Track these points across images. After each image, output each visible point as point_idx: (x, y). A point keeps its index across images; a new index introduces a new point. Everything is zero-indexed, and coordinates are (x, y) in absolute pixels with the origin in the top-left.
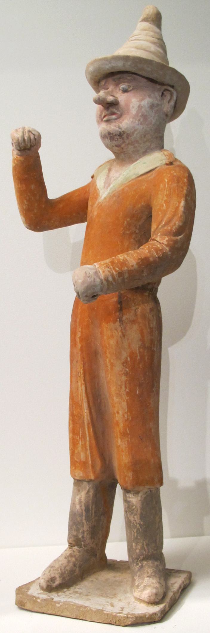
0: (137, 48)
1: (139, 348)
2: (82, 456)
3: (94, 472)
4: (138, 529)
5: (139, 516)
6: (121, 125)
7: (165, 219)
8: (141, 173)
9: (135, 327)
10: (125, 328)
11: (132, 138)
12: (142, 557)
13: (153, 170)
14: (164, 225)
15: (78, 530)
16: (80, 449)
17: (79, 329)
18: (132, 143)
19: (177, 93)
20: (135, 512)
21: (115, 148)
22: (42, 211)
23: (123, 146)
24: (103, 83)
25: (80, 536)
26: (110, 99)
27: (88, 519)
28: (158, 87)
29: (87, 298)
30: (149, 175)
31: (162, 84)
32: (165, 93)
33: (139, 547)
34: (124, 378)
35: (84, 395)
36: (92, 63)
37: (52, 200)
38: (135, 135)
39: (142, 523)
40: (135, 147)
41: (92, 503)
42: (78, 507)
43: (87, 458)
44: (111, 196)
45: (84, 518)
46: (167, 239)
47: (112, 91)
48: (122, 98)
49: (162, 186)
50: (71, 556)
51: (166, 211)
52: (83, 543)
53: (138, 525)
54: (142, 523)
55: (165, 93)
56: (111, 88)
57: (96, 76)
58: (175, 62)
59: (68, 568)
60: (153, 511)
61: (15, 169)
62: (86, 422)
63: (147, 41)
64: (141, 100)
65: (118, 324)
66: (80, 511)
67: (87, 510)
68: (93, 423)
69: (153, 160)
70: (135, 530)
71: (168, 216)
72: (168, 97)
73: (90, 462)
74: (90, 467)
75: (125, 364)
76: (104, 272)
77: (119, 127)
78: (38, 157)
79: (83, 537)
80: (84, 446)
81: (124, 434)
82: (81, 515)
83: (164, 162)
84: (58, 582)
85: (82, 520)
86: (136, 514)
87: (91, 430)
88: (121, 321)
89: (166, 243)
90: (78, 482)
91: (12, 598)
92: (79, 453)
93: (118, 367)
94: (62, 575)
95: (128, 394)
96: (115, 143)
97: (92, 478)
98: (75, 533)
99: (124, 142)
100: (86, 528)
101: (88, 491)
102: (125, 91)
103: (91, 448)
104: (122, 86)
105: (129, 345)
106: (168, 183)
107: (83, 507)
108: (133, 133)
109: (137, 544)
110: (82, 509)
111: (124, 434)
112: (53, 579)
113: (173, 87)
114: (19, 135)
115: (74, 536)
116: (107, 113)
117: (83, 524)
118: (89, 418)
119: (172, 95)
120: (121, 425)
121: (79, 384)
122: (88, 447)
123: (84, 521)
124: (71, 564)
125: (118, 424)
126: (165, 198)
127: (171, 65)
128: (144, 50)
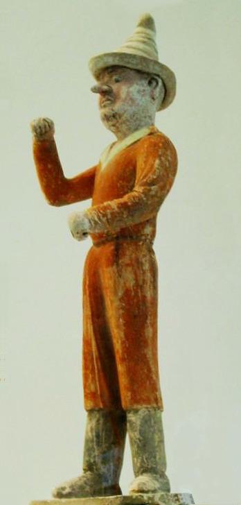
0: (128, 47)
1: (133, 286)
2: (92, 388)
3: (103, 402)
5: (138, 432)
6: (114, 108)
7: (144, 175)
9: (130, 269)
10: (121, 271)
11: (123, 118)
12: (142, 469)
13: (138, 140)
15: (90, 455)
16: (90, 381)
18: (124, 122)
21: (112, 128)
22: (59, 189)
23: (117, 125)
24: (101, 77)
25: (92, 461)
26: (105, 88)
27: (99, 444)
29: (79, 235)
31: (148, 74)
33: (139, 460)
34: (121, 312)
35: (92, 334)
38: (125, 115)
39: (141, 438)
40: (128, 126)
41: (103, 430)
42: (90, 434)
43: (96, 388)
44: (109, 165)
45: (95, 443)
46: (143, 188)
47: (107, 82)
48: (115, 87)
49: (142, 150)
50: (84, 477)
51: (145, 167)
52: (95, 467)
53: (138, 441)
54: (141, 438)
56: (106, 79)
58: (167, 56)
59: (79, 483)
60: (152, 430)
61: (35, 152)
64: (129, 88)
65: (114, 267)
66: (91, 437)
67: (98, 436)
68: (100, 357)
69: (142, 133)
70: (136, 446)
72: (154, 84)
73: (99, 393)
74: (99, 397)
75: (121, 300)
76: (91, 213)
77: (113, 110)
78: (53, 141)
79: (95, 462)
80: (93, 378)
81: (123, 360)
82: (92, 441)
84: (68, 490)
85: (93, 446)
86: (136, 431)
88: (118, 265)
89: (141, 191)
90: (91, 411)
92: (89, 385)
93: (117, 303)
94: (72, 487)
95: (125, 325)
96: (111, 123)
97: (102, 406)
98: (87, 459)
99: (118, 122)
100: (96, 453)
101: (98, 421)
102: (117, 81)
103: (99, 381)
104: (115, 77)
105: (125, 283)
106: (147, 148)
107: (94, 434)
108: (123, 114)
109: (137, 458)
110: (92, 436)
111: (123, 360)
112: (63, 489)
114: (35, 123)
115: (87, 461)
118: (97, 353)
119: (157, 83)
120: (120, 351)
121: (89, 325)
122: (97, 379)
123: (95, 447)
124: (82, 482)
125: (118, 352)
126: (144, 159)
127: (161, 61)
128: (134, 48)
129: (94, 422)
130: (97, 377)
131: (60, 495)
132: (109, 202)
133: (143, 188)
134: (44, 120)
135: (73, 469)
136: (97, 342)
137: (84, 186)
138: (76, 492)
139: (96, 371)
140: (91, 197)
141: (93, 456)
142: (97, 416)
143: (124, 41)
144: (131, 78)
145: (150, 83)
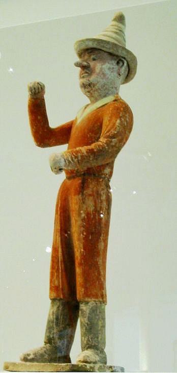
0: (104, 35)
1: (93, 212)
2: (56, 283)
3: (63, 294)
4: (86, 328)
5: (87, 318)
6: (90, 79)
7: (107, 130)
8: (98, 107)
9: (91, 198)
10: (85, 199)
11: (96, 87)
12: (87, 346)
13: (106, 104)
14: (107, 132)
15: (50, 333)
16: (55, 278)
17: (60, 201)
18: (97, 90)
19: (127, 61)
20: (85, 316)
21: (87, 93)
22: (45, 135)
23: (91, 92)
24: (82, 55)
25: (51, 336)
26: (85, 64)
27: (57, 324)
28: (115, 57)
29: (56, 170)
30: (104, 107)
31: (117, 56)
32: (120, 62)
34: (82, 229)
35: (60, 243)
36: (76, 44)
37: (53, 129)
38: (98, 85)
40: (99, 93)
41: (61, 315)
42: (51, 317)
43: (59, 283)
44: (83, 121)
45: (54, 324)
46: (106, 139)
47: (87, 60)
48: (92, 64)
49: (108, 112)
50: (44, 347)
51: (109, 125)
52: (53, 341)
55: (120, 62)
56: (86, 57)
57: (79, 51)
58: (131, 45)
59: (40, 352)
60: (97, 317)
61: (29, 107)
63: (112, 32)
64: (102, 65)
65: (80, 195)
66: (52, 319)
67: (57, 319)
68: (64, 261)
69: (109, 99)
70: (84, 328)
71: (109, 128)
72: (121, 64)
73: (61, 287)
74: (61, 290)
75: (83, 220)
76: (66, 155)
77: (89, 80)
78: (44, 100)
79: (53, 337)
80: (58, 276)
81: (81, 264)
82: (53, 322)
83: (113, 100)
84: (32, 356)
85: (53, 325)
86: (85, 317)
87: (63, 266)
88: (83, 194)
89: (105, 142)
90: (53, 300)
91: (3, 366)
92: (54, 280)
93: (80, 222)
94: (35, 354)
95: (84, 239)
96: (87, 90)
97: (62, 297)
99: (92, 89)
100: (55, 331)
101: (58, 307)
102: (94, 60)
103: (62, 278)
105: (87, 208)
106: (112, 110)
107: (55, 317)
108: (96, 84)
109: (85, 338)
111: (81, 264)
112: (29, 355)
113: (125, 58)
114: (31, 85)
115: (48, 337)
116: (83, 72)
117: (54, 327)
118: (62, 258)
119: (123, 64)
120: (79, 258)
121: (58, 237)
122: (60, 277)
123: (54, 326)
124: (43, 351)
125: (77, 257)
126: (109, 119)
127: (126, 48)
128: (109, 36)
129: (55, 308)
130: (60, 275)
131: (25, 359)
132: (81, 148)
133: (106, 139)
134: (38, 83)
135: (37, 341)
136: (62, 250)
137: (63, 134)
138: (37, 358)
139: (60, 271)
140: (68, 143)
141: (52, 333)
142: (58, 304)
143: (102, 31)
144: (105, 58)
145: (118, 63)
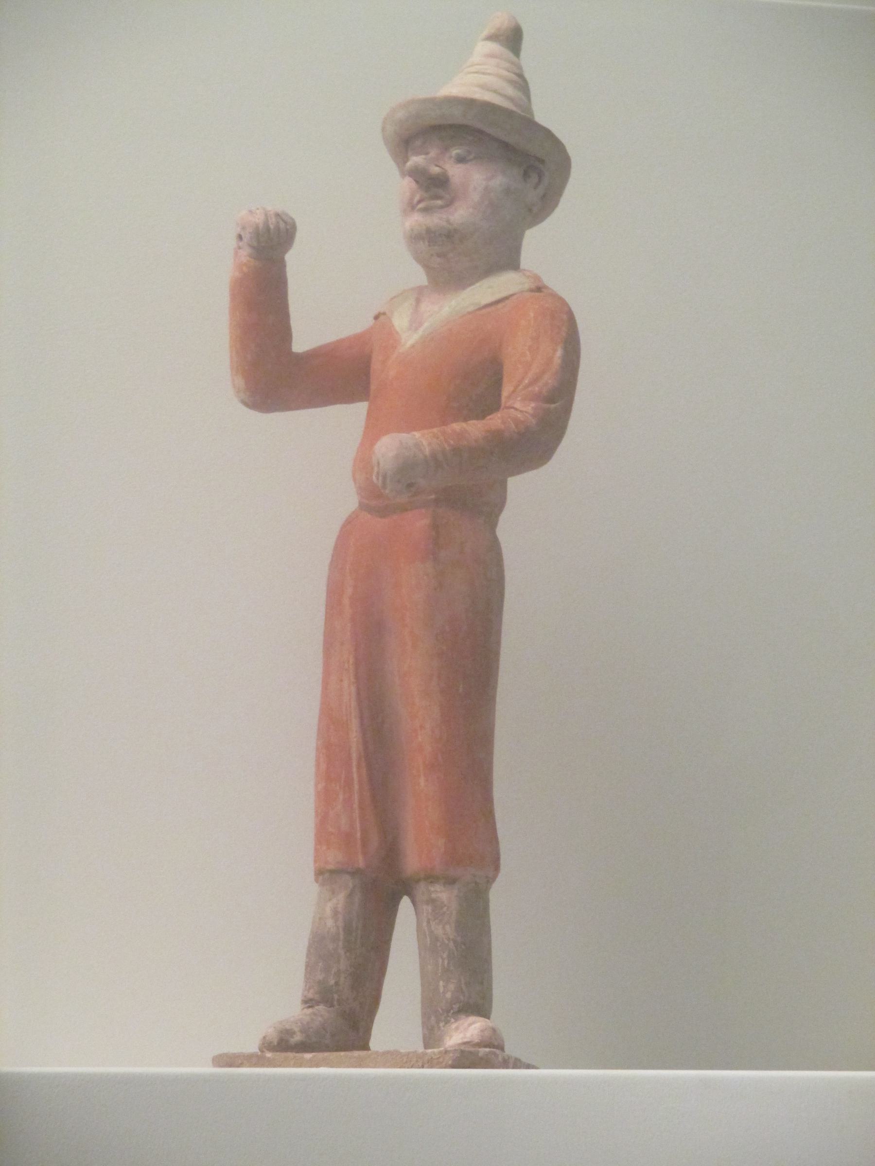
0: (484, 87)
6: (452, 218)
7: (530, 375)
14: (531, 384)
22: (280, 370)
26: (435, 170)
30: (500, 306)
33: (452, 987)
35: (354, 704)
39: (459, 939)
42: (330, 923)
45: (341, 943)
46: (533, 405)
48: (455, 172)
52: (336, 996)
53: (451, 944)
54: (459, 939)
56: (433, 153)
62: (354, 756)
67: (348, 929)
70: (445, 955)
72: (534, 178)
73: (359, 835)
76: (430, 444)
77: (448, 221)
79: (337, 984)
84: (298, 1038)
89: (531, 411)
97: (361, 862)
98: (320, 977)
100: (343, 965)
101: (350, 896)
102: (461, 160)
104: (455, 152)
107: (341, 924)
110: (338, 927)
112: (290, 1032)
115: (319, 982)
121: (346, 683)
122: (356, 806)
123: (341, 952)
128: (495, 91)
129: (341, 898)
130: (356, 797)
131: (267, 1045)
132: (464, 425)
133: (533, 405)
134: (277, 215)
135: (282, 996)
136: (362, 724)
137: (340, 374)
138: (285, 1045)
139: (356, 787)
140: (366, 400)
141: (334, 970)
142: (351, 885)
143: (472, 76)
144: (490, 159)
145: (526, 175)
